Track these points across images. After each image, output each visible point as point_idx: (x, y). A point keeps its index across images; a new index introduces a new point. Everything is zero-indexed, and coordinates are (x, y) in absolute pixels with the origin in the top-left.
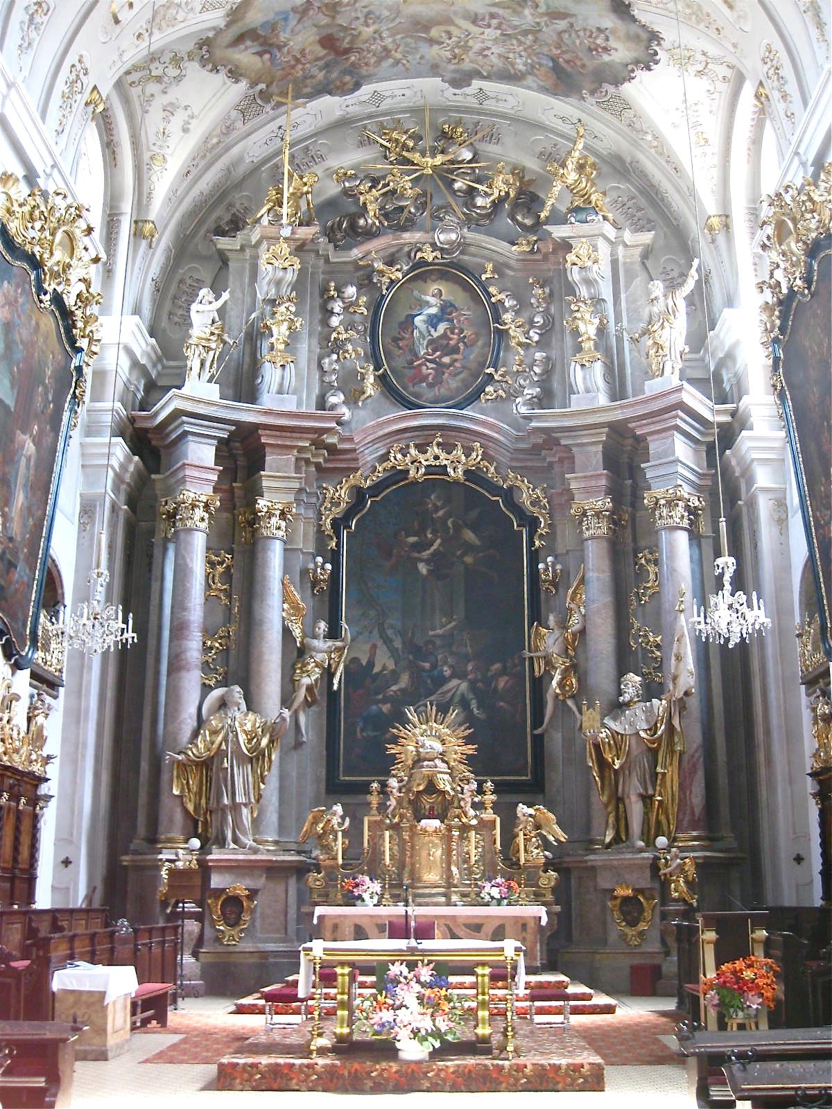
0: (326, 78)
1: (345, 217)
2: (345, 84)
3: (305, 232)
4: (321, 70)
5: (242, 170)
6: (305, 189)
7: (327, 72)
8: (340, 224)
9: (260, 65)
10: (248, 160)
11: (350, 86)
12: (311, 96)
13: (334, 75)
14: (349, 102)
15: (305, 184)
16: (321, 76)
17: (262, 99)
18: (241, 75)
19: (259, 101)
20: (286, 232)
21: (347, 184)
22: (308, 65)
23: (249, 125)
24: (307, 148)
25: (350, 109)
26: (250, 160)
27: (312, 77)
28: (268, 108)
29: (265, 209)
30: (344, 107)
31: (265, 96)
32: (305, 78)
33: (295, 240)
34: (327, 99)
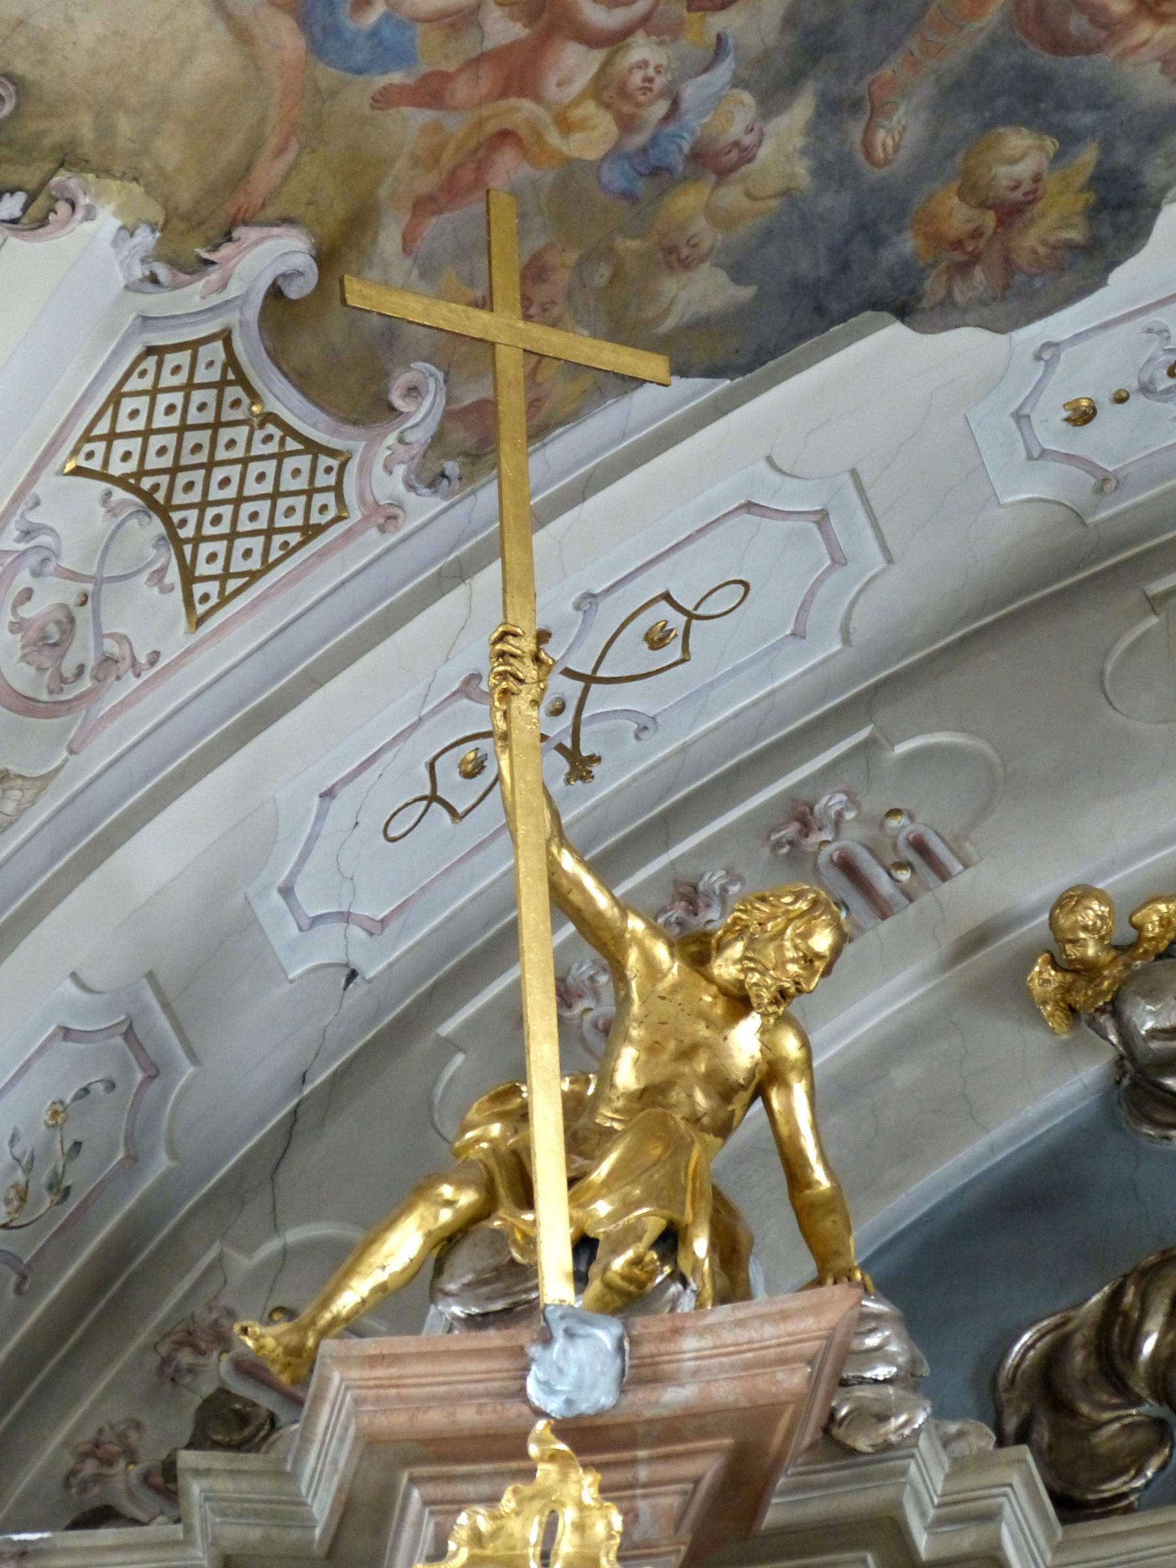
0: (832, 170)
1: (1148, 1277)
2: (1011, 212)
3: (739, 1349)
4: (774, 92)
5: (249, 1063)
6: (744, 1044)
7: (833, 109)
8: (1114, 1335)
9: (213, 60)
10: (304, 956)
11: (1059, 220)
12: (737, 355)
13: (899, 133)
14: (1091, 372)
15: (739, 1002)
16: (783, 144)
17: (302, 381)
18: (68, 158)
19: (283, 399)
20: (576, 1370)
21: (1147, 1019)
22: (641, 50)
23: (242, 636)
24: (802, 814)
25: (1112, 440)
26: (328, 947)
27: (714, 162)
28: (381, 467)
29: (402, 1245)
30: (1050, 427)
31: (325, 349)
32: (656, 170)
33: (674, 1431)
34: (880, 371)
